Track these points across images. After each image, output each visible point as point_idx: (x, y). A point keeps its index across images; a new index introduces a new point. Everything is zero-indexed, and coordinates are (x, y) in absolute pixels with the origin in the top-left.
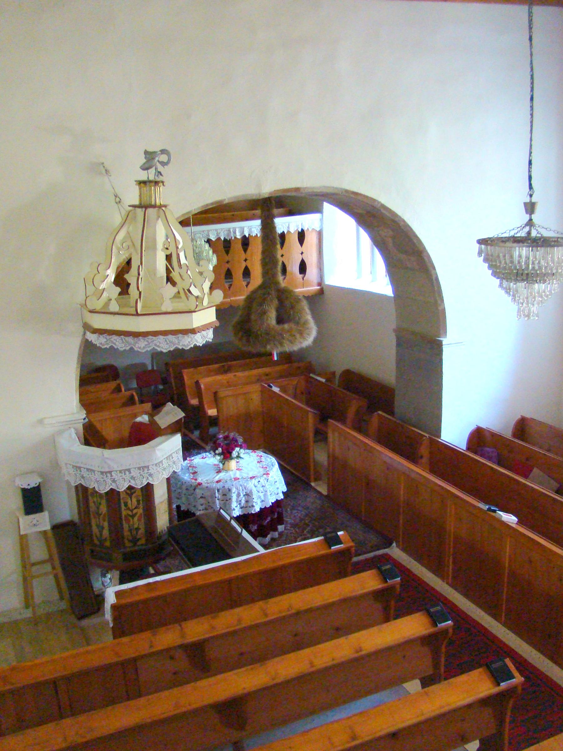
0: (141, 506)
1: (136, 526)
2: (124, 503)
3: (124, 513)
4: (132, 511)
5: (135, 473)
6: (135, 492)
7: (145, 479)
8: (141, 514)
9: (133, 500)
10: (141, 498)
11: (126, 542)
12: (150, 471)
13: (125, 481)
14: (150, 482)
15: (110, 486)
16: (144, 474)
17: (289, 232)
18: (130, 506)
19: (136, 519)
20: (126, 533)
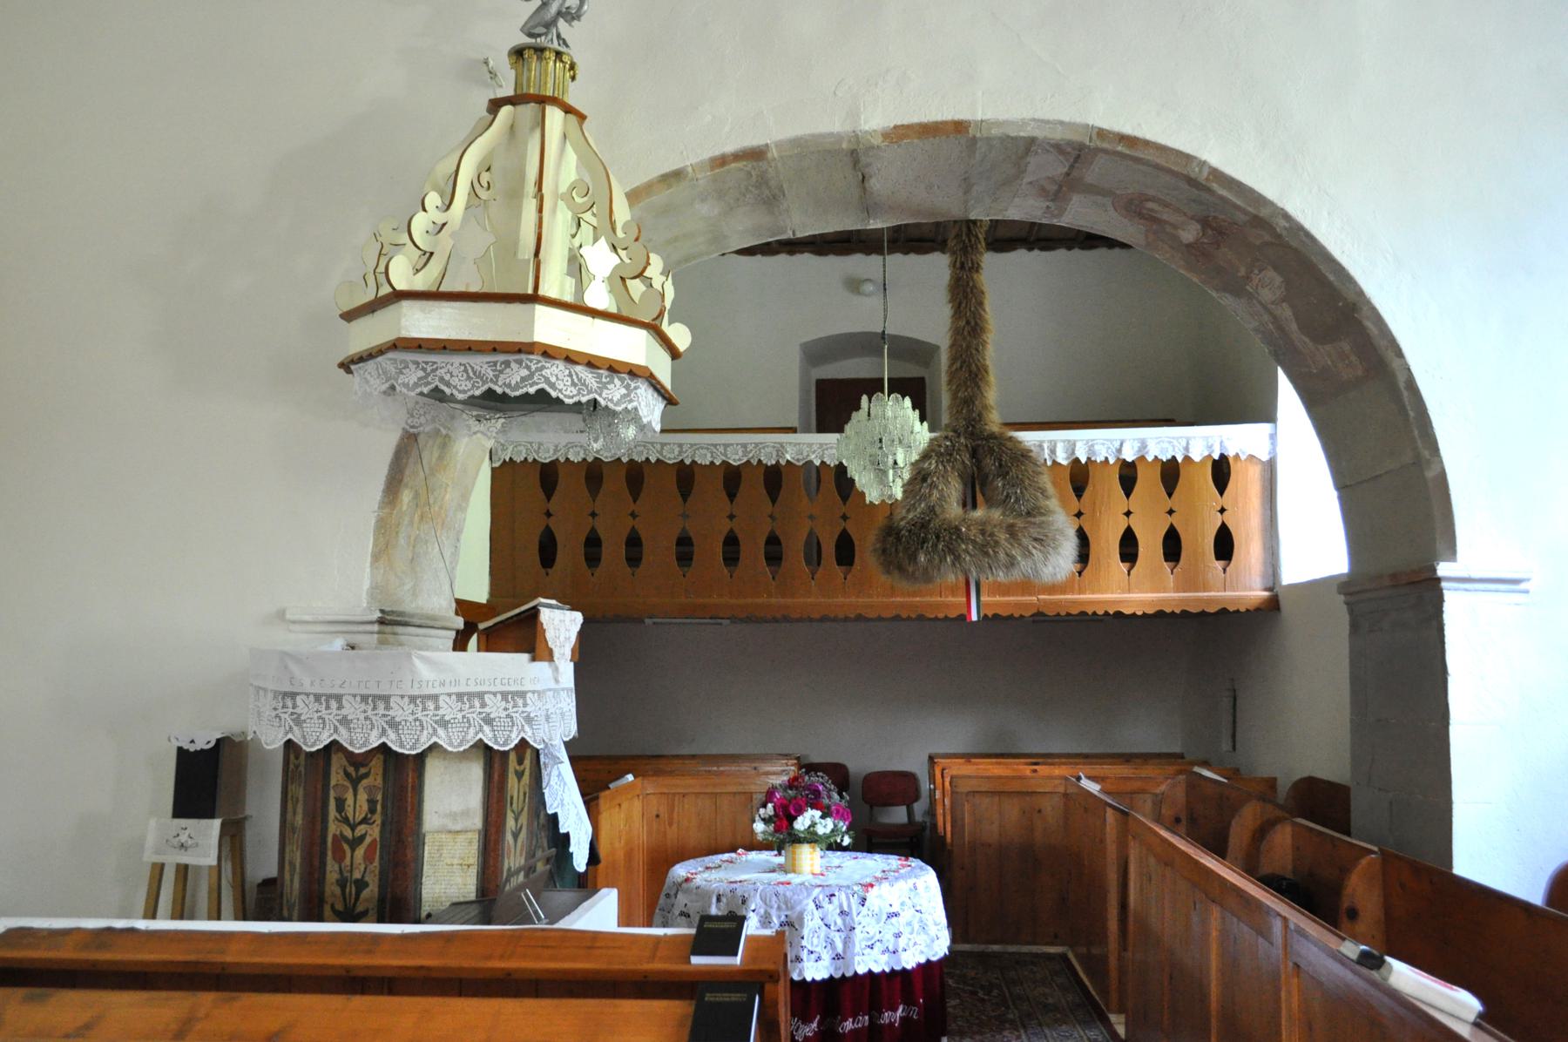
0: (378, 818)
1: (357, 875)
2: (335, 798)
3: (333, 828)
4: (353, 829)
5: (352, 709)
6: (366, 775)
7: (375, 733)
8: (374, 841)
9: (359, 797)
10: (379, 797)
12: (391, 713)
13: (324, 723)
14: (390, 744)
16: (374, 718)
19: (360, 852)
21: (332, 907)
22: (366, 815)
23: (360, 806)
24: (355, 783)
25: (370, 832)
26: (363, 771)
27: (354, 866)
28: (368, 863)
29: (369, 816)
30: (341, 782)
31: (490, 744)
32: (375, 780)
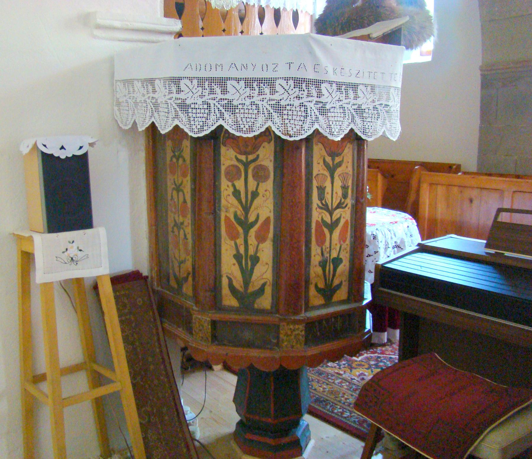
1: (334, 254)
2: (317, 187)
3: (316, 215)
4: (331, 214)
6: (340, 164)
11: (312, 291)
15: (313, 123)
17: (285, 9)
18: (328, 197)
19: (336, 233)
20: (315, 270)
21: (316, 286)
22: (341, 200)
23: (336, 193)
24: (332, 171)
25: (343, 215)
26: (337, 160)
27: (332, 247)
28: (342, 243)
29: (343, 200)
30: (322, 172)
31: (359, 134)
32: (347, 167)
